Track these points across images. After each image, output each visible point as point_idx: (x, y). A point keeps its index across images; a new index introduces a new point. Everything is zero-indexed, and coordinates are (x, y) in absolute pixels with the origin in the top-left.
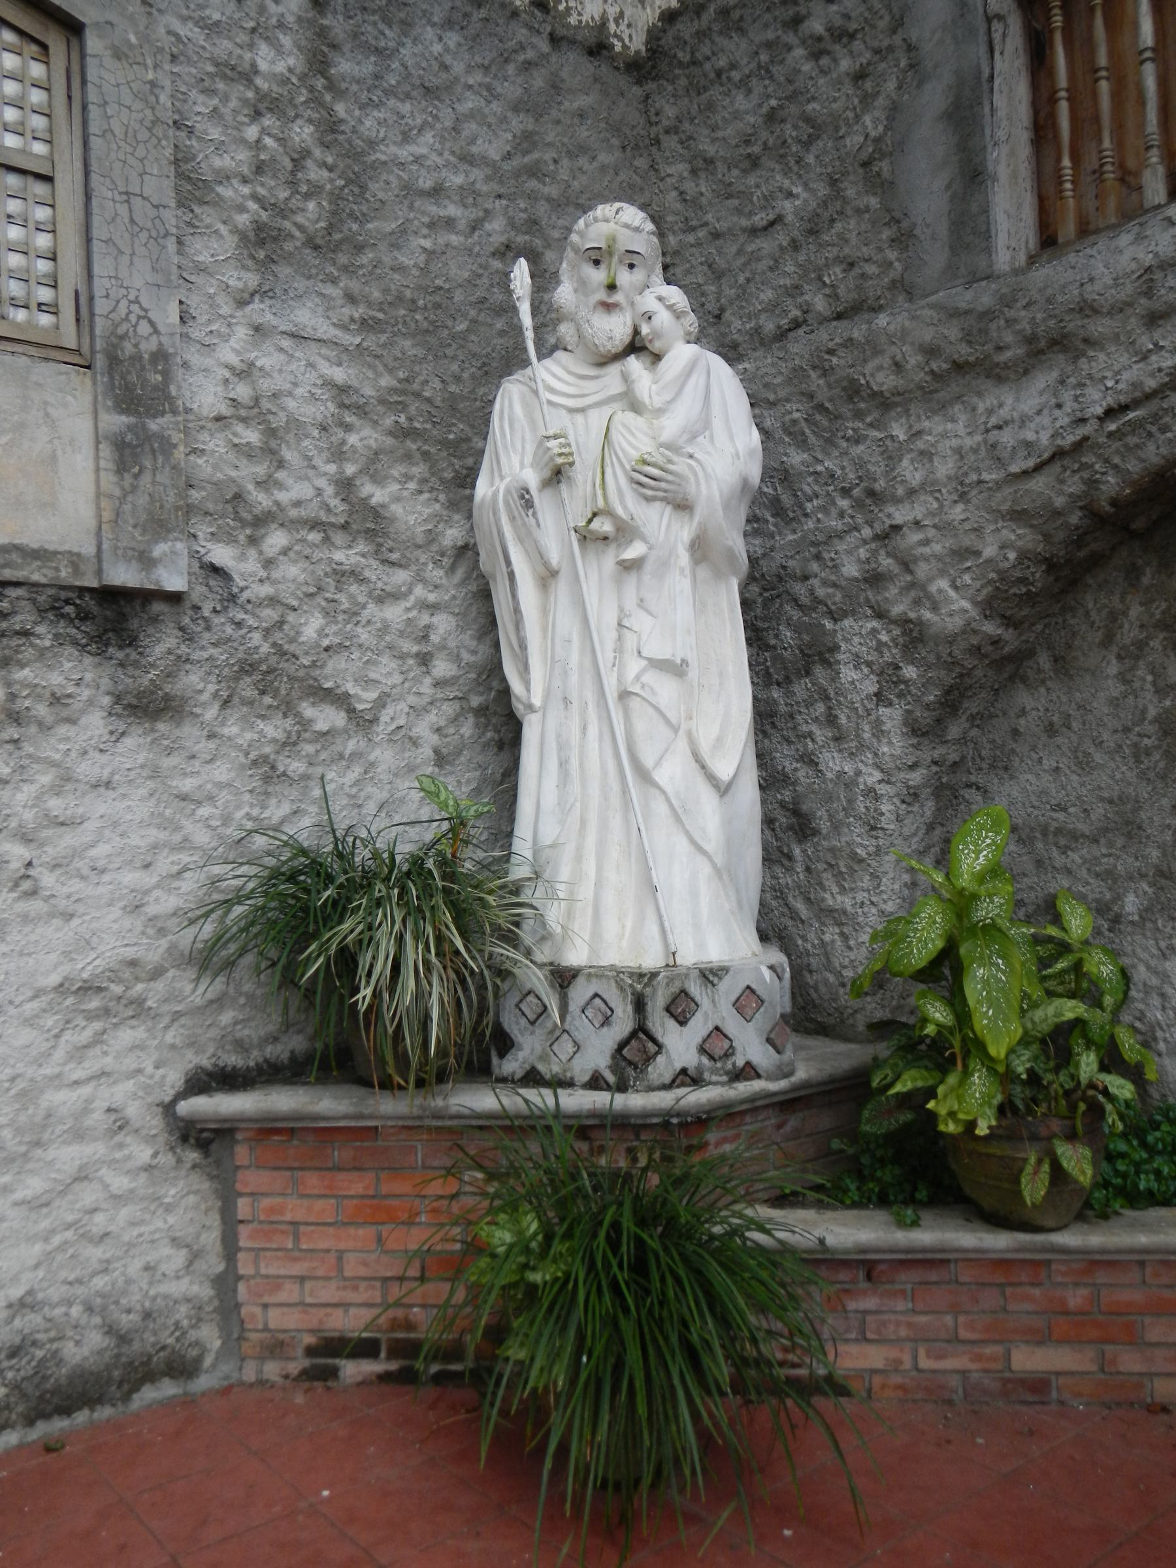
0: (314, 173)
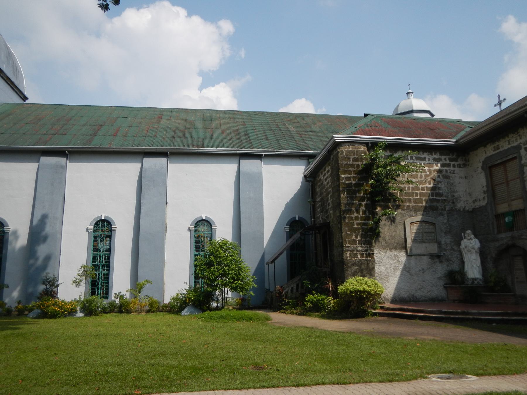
0: (448, 228)
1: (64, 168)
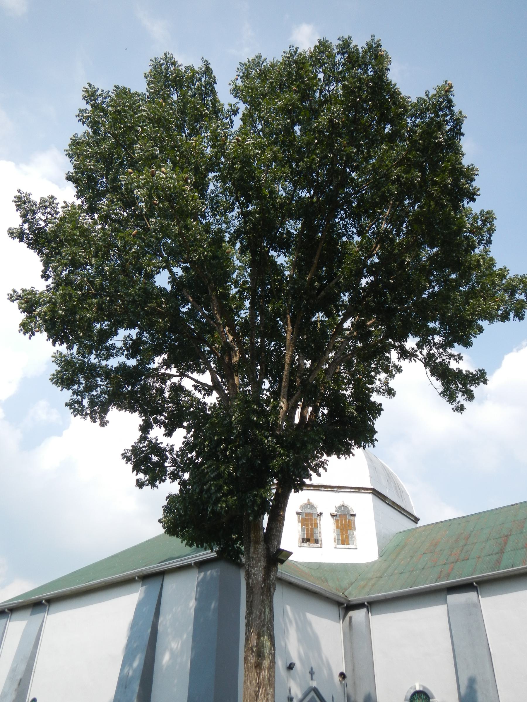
1: (477, 606)
